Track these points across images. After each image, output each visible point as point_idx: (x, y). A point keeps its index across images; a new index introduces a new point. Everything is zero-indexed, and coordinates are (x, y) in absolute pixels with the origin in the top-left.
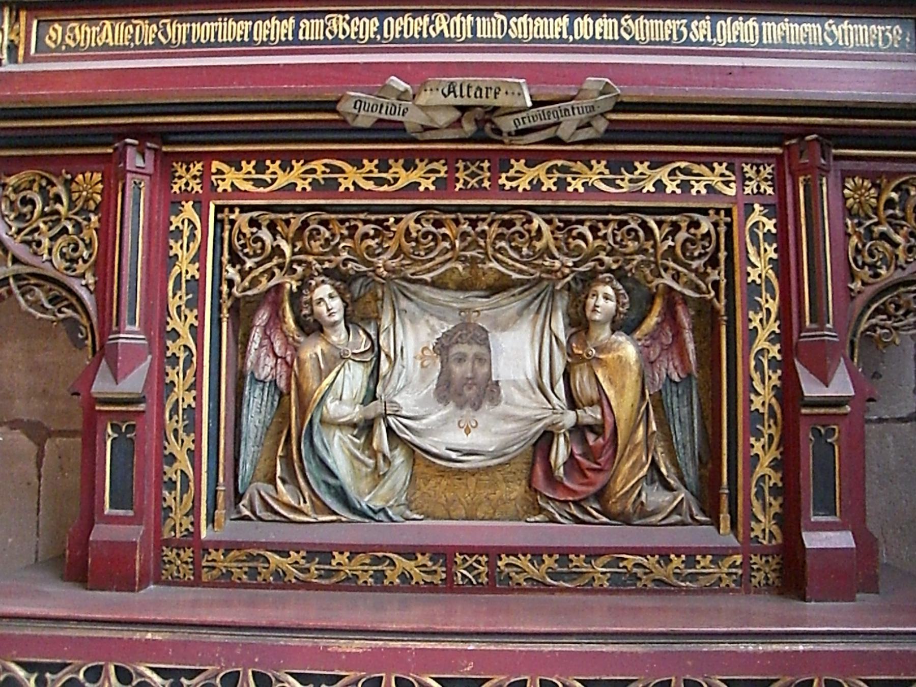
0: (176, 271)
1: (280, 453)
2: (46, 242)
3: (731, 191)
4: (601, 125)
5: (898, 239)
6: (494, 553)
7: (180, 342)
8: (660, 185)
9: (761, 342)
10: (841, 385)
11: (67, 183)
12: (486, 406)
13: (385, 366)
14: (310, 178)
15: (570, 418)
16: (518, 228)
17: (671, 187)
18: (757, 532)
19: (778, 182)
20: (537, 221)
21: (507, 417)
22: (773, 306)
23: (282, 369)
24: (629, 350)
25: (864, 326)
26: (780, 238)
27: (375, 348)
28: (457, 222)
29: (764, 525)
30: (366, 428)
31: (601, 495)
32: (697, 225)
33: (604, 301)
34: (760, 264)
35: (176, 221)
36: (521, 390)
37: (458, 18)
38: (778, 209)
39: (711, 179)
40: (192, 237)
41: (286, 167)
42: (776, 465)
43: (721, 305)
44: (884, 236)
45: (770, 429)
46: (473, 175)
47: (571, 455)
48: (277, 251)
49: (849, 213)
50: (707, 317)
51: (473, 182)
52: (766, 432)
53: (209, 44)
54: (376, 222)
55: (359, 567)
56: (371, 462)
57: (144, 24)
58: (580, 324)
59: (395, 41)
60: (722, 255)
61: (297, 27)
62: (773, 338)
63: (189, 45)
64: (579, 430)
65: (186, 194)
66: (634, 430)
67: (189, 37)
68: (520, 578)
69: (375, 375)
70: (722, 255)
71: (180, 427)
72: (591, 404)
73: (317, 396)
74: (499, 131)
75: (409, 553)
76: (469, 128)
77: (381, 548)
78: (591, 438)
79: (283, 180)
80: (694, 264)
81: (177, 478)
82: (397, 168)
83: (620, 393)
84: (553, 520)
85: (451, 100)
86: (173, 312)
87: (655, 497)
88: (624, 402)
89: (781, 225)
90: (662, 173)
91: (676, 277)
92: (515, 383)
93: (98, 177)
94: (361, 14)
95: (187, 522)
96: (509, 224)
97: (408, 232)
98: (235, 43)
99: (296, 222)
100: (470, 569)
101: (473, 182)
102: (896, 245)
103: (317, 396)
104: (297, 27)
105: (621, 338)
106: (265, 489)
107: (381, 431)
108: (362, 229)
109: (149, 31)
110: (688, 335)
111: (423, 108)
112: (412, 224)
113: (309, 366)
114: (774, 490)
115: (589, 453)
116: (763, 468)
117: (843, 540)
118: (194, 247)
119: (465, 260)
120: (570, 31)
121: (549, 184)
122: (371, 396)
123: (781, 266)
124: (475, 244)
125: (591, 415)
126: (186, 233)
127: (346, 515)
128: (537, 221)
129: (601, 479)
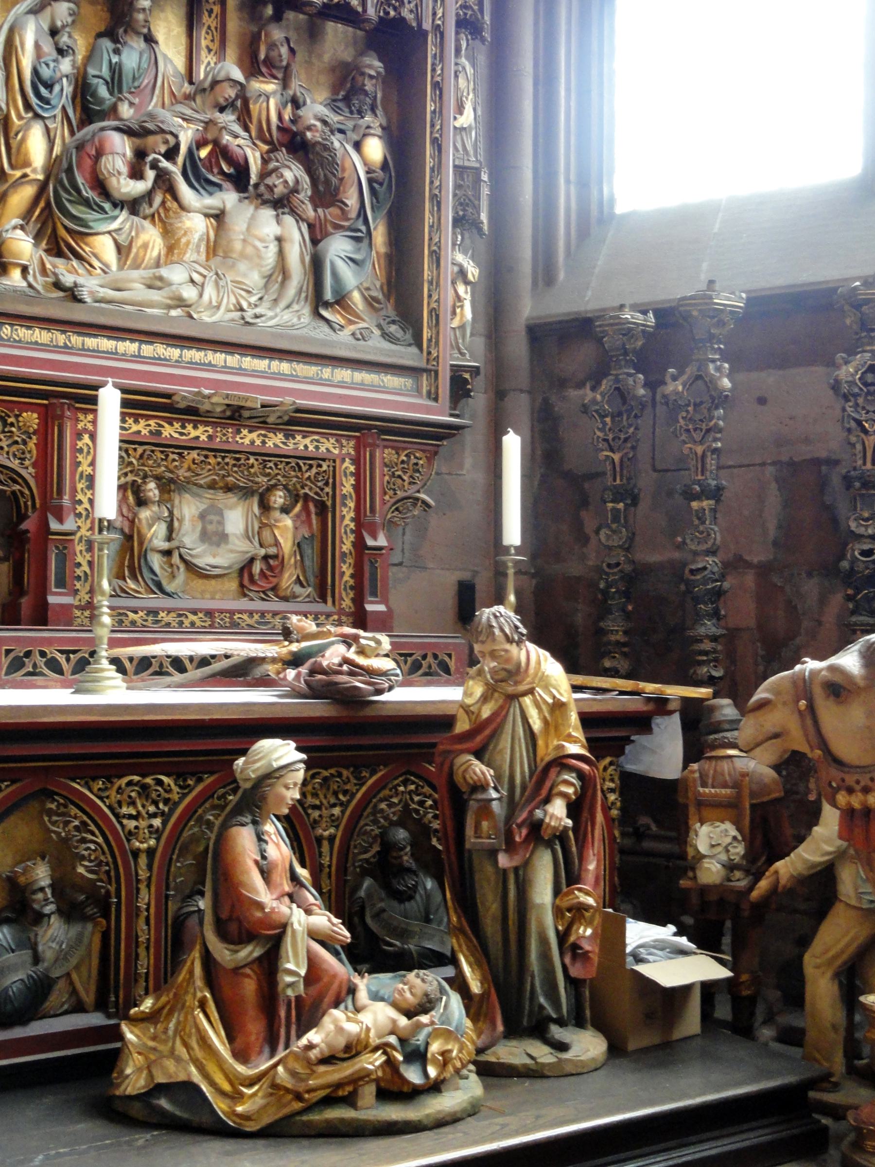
0: (80, 469)
1: (126, 563)
2: (6, 449)
3: (336, 452)
4: (286, 418)
5: (405, 478)
6: (232, 613)
7: (84, 506)
8: (306, 447)
9: (347, 521)
10: (382, 541)
11: (17, 416)
12: (223, 545)
13: (176, 524)
14: (148, 428)
15: (263, 552)
16: (242, 461)
17: (311, 448)
18: (344, 606)
19: (357, 449)
20: (252, 460)
21: (232, 551)
22: (352, 505)
23: (126, 523)
24: (288, 522)
25: (389, 516)
26: (357, 475)
27: (171, 513)
28: (215, 457)
29: (347, 603)
30: (168, 553)
31: (274, 589)
32: (320, 466)
33: (279, 498)
34: (347, 486)
35: (80, 444)
36: (238, 538)
37: (218, 354)
38: (356, 461)
39: (328, 446)
40: (88, 453)
41: (136, 421)
42: (352, 576)
43: (329, 503)
44: (399, 477)
45: (350, 560)
46: (224, 435)
47: (262, 570)
48: (131, 463)
49: (386, 465)
50: (322, 509)
51: (224, 438)
52: (348, 561)
53: (94, 351)
54: (178, 453)
55: (170, 618)
56: (169, 570)
57: (58, 334)
58: (265, 507)
59: (188, 363)
60: (331, 481)
61: (140, 348)
62: (352, 520)
63: (83, 349)
64: (266, 558)
65: (85, 430)
66: (290, 559)
67: (83, 344)
68: (243, 624)
69: (171, 529)
70: (331, 481)
71: (83, 549)
72: (270, 546)
73: (149, 536)
74: (240, 416)
75: (194, 612)
76: (228, 413)
77: (182, 609)
78: (271, 562)
79: (135, 428)
80: (319, 484)
81: (82, 575)
82: (190, 427)
83: (285, 541)
84: (252, 600)
85: (227, 402)
86: (79, 490)
87: (298, 589)
88: (287, 545)
89: (358, 469)
90: (307, 441)
91: (311, 489)
92: (235, 535)
93: (35, 415)
94: (173, 346)
95: (87, 597)
96: (238, 459)
97: (194, 460)
98: (107, 352)
99: (140, 450)
100: (222, 619)
101: (224, 438)
102: (404, 480)
103: (149, 536)
104: (140, 348)
105: (284, 516)
106: (121, 583)
107: (176, 555)
108: (172, 456)
109: (61, 339)
110: (313, 517)
111: (212, 404)
112: (196, 456)
113: (144, 522)
114: (352, 588)
115: (271, 568)
116: (346, 578)
117: (382, 608)
118: (90, 458)
119: (218, 475)
120: (269, 368)
121: (258, 442)
122: (169, 538)
123: (357, 487)
124: (223, 469)
125: (272, 551)
126: (85, 450)
127: (161, 595)
128: (252, 460)
129: (275, 580)
